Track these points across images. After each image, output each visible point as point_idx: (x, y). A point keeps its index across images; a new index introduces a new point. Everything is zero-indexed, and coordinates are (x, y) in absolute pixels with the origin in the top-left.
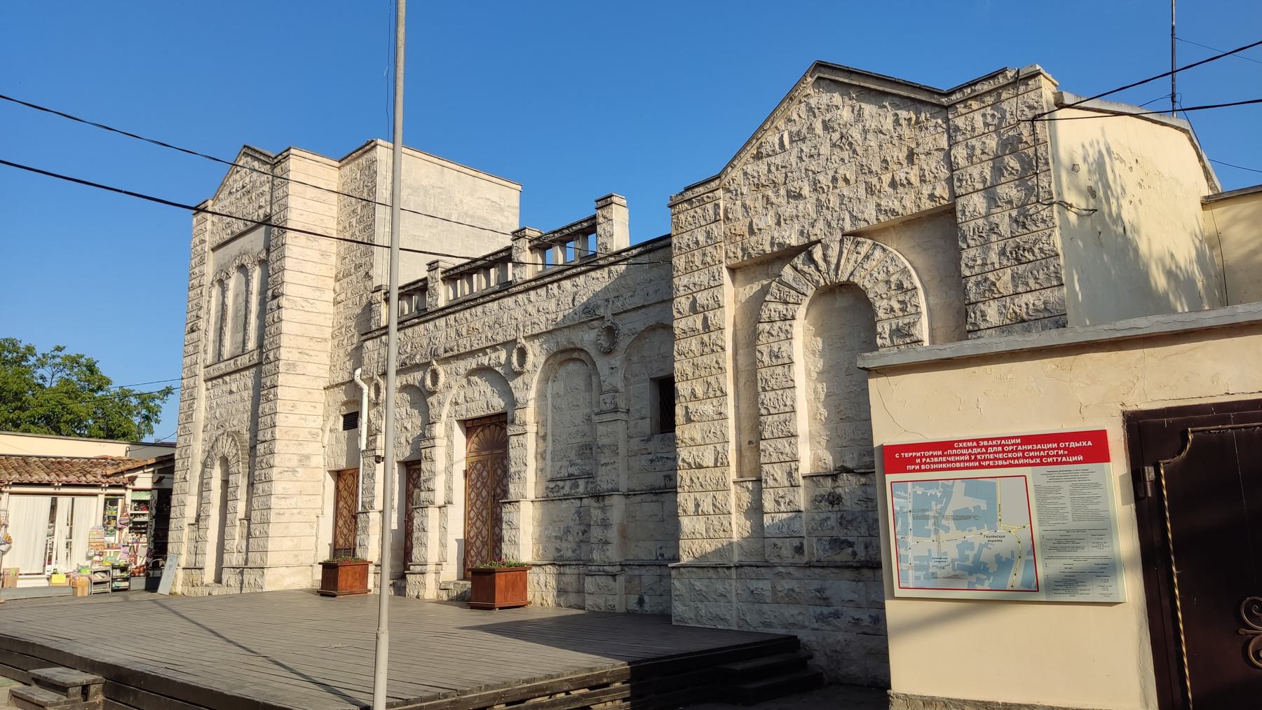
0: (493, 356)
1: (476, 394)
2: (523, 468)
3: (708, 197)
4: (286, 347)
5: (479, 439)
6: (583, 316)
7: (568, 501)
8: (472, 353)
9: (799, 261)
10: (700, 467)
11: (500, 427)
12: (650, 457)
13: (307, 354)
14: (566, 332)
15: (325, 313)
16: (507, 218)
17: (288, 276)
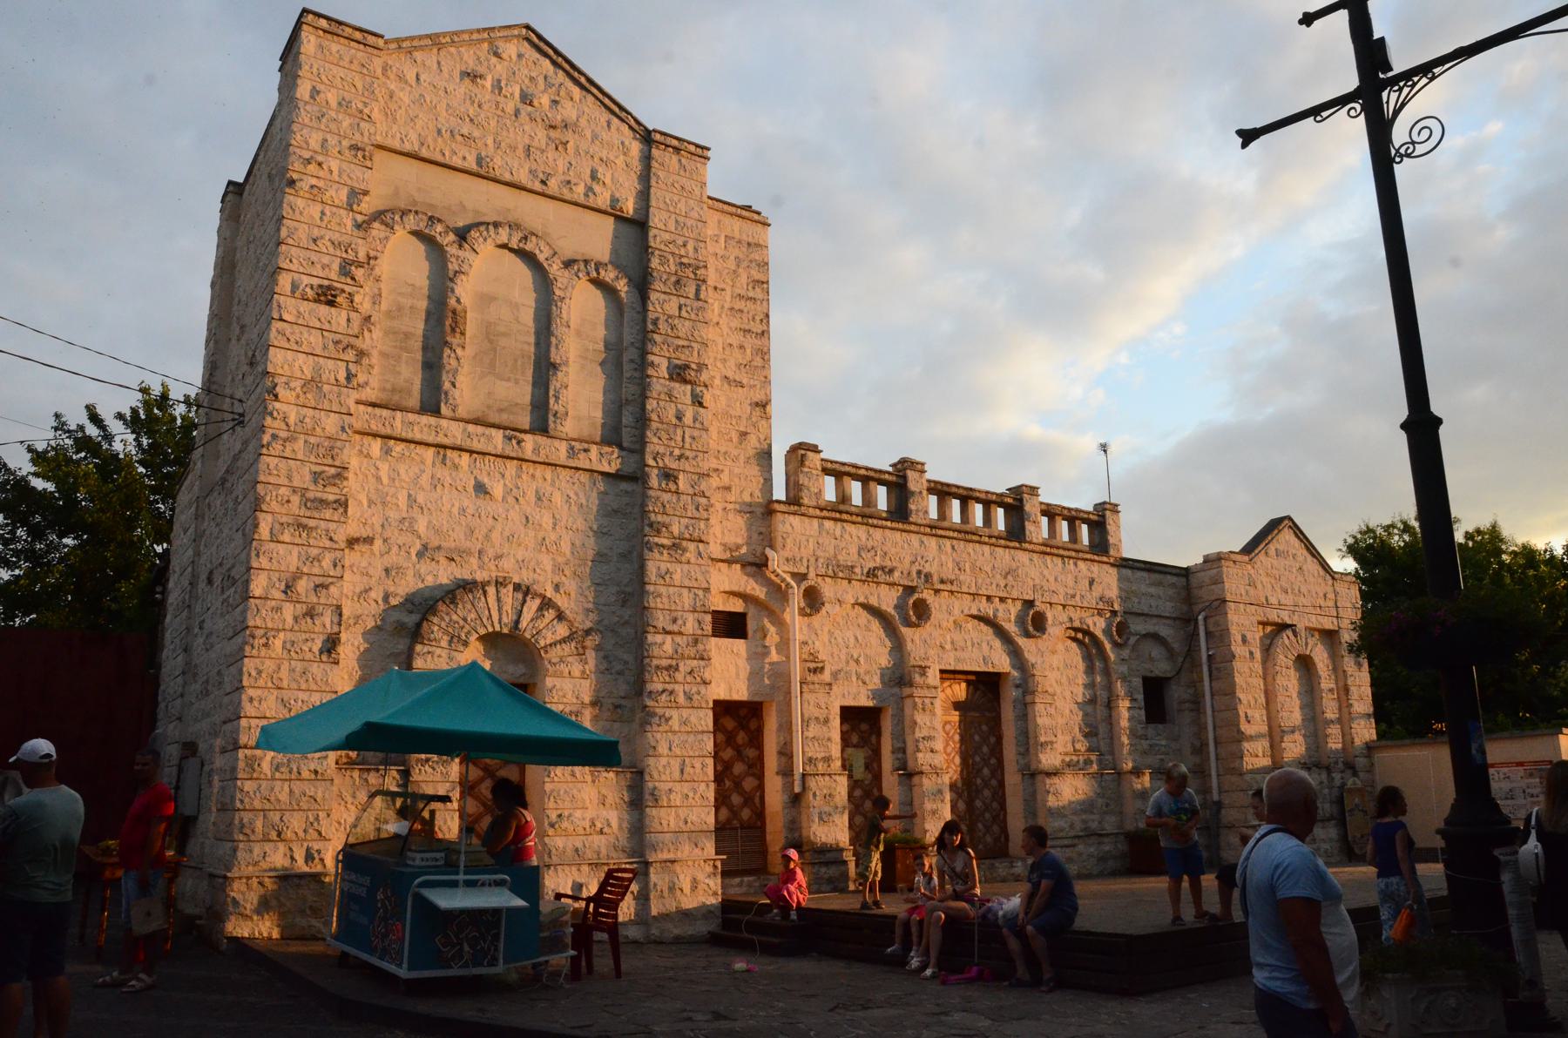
0: (1001, 607)
9: (1289, 632)
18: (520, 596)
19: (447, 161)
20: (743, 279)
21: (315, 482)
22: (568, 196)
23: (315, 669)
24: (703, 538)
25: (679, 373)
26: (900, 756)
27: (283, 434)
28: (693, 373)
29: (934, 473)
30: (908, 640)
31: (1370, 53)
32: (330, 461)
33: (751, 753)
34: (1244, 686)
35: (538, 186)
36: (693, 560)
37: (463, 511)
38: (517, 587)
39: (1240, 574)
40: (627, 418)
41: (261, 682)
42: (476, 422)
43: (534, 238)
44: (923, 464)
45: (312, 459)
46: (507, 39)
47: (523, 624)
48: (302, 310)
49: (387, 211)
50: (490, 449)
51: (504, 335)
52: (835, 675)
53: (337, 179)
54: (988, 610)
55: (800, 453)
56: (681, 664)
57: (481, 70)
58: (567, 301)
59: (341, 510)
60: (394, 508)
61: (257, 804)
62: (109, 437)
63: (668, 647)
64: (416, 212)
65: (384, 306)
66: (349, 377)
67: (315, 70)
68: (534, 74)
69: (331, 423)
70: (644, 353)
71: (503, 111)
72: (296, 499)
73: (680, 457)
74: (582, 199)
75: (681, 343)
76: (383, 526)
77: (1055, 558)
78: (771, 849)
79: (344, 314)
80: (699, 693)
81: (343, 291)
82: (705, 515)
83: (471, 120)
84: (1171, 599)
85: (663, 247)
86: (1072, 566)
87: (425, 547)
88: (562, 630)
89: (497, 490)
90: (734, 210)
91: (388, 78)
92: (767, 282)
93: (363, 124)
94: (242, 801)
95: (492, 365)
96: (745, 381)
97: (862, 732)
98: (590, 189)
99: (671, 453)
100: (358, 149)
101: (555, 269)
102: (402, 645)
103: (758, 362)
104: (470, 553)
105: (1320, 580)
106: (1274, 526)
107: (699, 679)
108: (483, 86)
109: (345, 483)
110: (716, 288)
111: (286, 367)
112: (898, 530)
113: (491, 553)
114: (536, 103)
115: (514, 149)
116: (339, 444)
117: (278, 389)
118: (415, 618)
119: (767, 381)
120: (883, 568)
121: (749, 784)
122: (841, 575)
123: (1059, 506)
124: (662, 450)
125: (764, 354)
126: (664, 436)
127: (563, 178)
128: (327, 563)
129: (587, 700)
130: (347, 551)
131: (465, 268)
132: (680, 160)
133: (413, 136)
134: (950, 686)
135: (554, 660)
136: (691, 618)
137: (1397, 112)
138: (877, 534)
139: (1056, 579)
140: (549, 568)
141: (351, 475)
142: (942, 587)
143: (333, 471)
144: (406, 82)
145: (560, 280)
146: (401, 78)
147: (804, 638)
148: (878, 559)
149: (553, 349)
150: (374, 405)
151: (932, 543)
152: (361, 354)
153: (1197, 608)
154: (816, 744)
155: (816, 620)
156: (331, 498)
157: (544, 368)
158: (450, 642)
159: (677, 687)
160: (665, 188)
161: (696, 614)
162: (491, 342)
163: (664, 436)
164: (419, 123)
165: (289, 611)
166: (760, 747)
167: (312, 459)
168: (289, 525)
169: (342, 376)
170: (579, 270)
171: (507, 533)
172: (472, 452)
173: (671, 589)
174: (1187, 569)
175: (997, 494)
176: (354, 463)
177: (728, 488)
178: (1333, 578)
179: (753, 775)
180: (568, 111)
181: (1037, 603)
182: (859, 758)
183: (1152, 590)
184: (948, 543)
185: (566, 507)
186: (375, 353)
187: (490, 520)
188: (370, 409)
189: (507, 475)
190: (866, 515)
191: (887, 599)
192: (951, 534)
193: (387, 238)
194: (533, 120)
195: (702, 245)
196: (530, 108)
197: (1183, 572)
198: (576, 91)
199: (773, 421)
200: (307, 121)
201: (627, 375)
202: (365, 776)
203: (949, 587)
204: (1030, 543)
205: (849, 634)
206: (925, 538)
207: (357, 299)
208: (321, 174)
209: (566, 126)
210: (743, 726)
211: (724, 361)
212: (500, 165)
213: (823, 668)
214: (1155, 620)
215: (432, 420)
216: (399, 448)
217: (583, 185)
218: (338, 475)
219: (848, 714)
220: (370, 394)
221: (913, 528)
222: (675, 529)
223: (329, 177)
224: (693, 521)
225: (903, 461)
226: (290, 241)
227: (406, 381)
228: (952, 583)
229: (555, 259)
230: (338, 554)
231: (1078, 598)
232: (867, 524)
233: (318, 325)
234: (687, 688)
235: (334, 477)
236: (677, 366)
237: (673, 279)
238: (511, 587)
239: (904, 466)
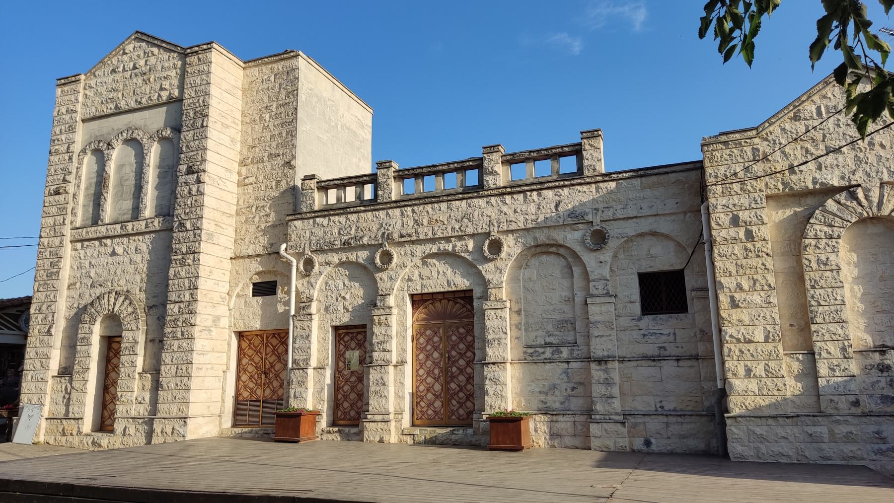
0: (459, 244)
1: (435, 274)
2: (503, 336)
3: (745, 142)
4: (206, 218)
5: (429, 311)
6: (569, 219)
7: (552, 364)
8: (433, 240)
10: (750, 342)
11: (454, 301)
12: (642, 332)
13: (220, 227)
14: (546, 231)
15: (232, 193)
16: (365, 133)
17: (209, 156)
22: (151, 103)
24: (197, 251)
25: (190, 171)
28: (196, 167)
32: (56, 256)
36: (191, 263)
41: (31, 346)
45: (51, 257)
50: (116, 234)
51: (127, 180)
54: (444, 246)
63: (176, 310)
71: (126, 78)
79: (63, 196)
89: (119, 250)
95: (122, 195)
97: (358, 340)
125: (292, 134)
134: (432, 304)
142: (403, 239)
143: (57, 260)
154: (300, 351)
159: (178, 329)
160: (191, 75)
161: (191, 291)
167: (51, 257)
171: (123, 269)
173: (180, 280)
181: (492, 234)
187: (117, 265)
189: (125, 243)
197: (698, 165)
203: (408, 239)
215: (96, 228)
216: (86, 243)
224: (192, 243)
233: (56, 204)
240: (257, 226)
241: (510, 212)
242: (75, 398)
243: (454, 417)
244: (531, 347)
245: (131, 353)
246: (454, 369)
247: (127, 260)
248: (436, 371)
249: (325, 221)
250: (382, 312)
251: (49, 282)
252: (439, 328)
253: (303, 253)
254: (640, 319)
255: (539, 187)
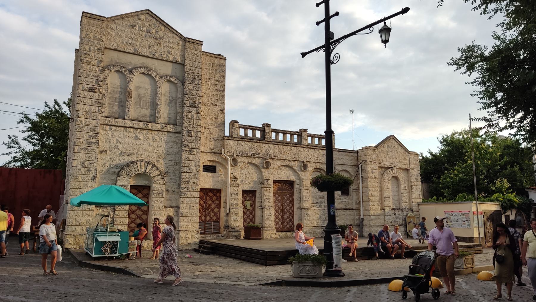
1: (283, 173)
9: (390, 170)
10: (374, 206)
18: (146, 164)
19: (126, 51)
20: (218, 75)
21: (90, 138)
22: (161, 58)
23: (90, 183)
25: (193, 106)
26: (260, 203)
27: (81, 126)
28: (196, 105)
29: (272, 127)
30: (264, 172)
31: (329, 35)
32: (94, 132)
33: (217, 202)
34: (371, 185)
35: (152, 56)
36: (195, 154)
37: (132, 143)
38: (146, 162)
39: (373, 153)
40: (178, 118)
42: (135, 120)
43: (151, 71)
44: (270, 125)
45: (89, 132)
46: (143, 14)
47: (147, 171)
48: (85, 94)
49: (109, 66)
50: (139, 127)
51: (143, 97)
52: (241, 182)
53: (94, 58)
54: (288, 163)
55: (233, 123)
56: (191, 180)
57: (135, 24)
58: (161, 87)
59: (97, 144)
60: (113, 143)
61: (74, 217)
62: (61, 109)
64: (117, 65)
65: (109, 91)
66: (99, 110)
67: (87, 29)
68: (150, 24)
69: (94, 122)
70: (183, 100)
71: (142, 35)
72: (85, 142)
73: (192, 128)
74: (165, 59)
75: (193, 97)
76: (109, 148)
77: (311, 149)
78: (221, 227)
79: (97, 94)
80: (196, 188)
81: (97, 88)
82: (199, 142)
83: (132, 38)
84: (351, 160)
85: (189, 71)
86: (317, 151)
87: (121, 152)
88: (158, 172)
90: (215, 56)
91: (108, 29)
92: (225, 76)
93: (101, 43)
94: (70, 216)
95: (140, 105)
96: (217, 104)
98: (167, 56)
99: (190, 127)
100: (100, 50)
101: (157, 78)
102: (115, 177)
103: (222, 99)
104: (133, 154)
105: (404, 154)
106: (389, 138)
107: (196, 184)
108: (136, 29)
109: (98, 138)
110: (209, 79)
111: (81, 109)
112: (261, 143)
113: (139, 153)
114: (151, 32)
115: (145, 46)
116: (96, 128)
117: (79, 114)
118: (118, 170)
119: (224, 104)
120: (256, 153)
121: (216, 210)
122: (243, 155)
123: (314, 134)
124: (187, 125)
125: (223, 96)
126: (188, 122)
127: (159, 53)
128: (93, 158)
129: (164, 190)
130: (99, 154)
131: (132, 80)
132: (194, 47)
133: (116, 44)
135: (155, 180)
136: (194, 168)
137: (332, 50)
138: (255, 144)
139: (311, 155)
140: (156, 157)
141: (100, 135)
142: (274, 158)
143: (95, 135)
144: (113, 29)
145: (159, 81)
146: (112, 29)
147: (232, 172)
148: (255, 151)
149: (157, 100)
150: (106, 117)
151: (272, 146)
152: (103, 104)
153: (359, 163)
155: (236, 168)
156: (94, 141)
157: (154, 105)
158: (127, 176)
159: (189, 186)
162: (140, 99)
163: (188, 122)
164: (117, 41)
165: (83, 170)
166: (220, 201)
167: (89, 132)
168: (83, 148)
169: (97, 110)
170: (164, 78)
171: (144, 148)
172: (134, 128)
174: (357, 151)
175: (293, 132)
176: (101, 132)
177: (212, 133)
178: (409, 153)
179: (217, 208)
180: (161, 34)
181: (305, 162)
182: (248, 203)
183: (345, 157)
184: (277, 146)
185: (161, 141)
186: (106, 104)
188: (105, 118)
189: (144, 133)
190: (253, 139)
191: (257, 161)
192: (278, 143)
193: (109, 73)
194: (150, 37)
195: (200, 69)
196: (149, 34)
197: (357, 152)
198: (163, 28)
199: (226, 115)
200: (85, 43)
201: (178, 106)
202: (103, 209)
203: (277, 158)
204: (303, 145)
205: (246, 171)
206: (270, 145)
207: (101, 90)
208: (89, 57)
209: (160, 39)
210: (215, 195)
211: (211, 99)
212: (142, 51)
213: (237, 180)
214: (345, 166)
215: (123, 121)
216: (114, 128)
217: (165, 55)
218: (96, 136)
219: (245, 192)
220: (105, 114)
221: (266, 142)
222: (191, 146)
223: (92, 58)
225: (264, 124)
226: (82, 76)
227: (116, 110)
228: (277, 157)
229: (158, 76)
230: (96, 155)
231: (318, 160)
232: (252, 142)
233: (90, 97)
234: (192, 186)
235: (95, 136)
236: (192, 103)
237: (191, 79)
238: (144, 162)
239: (266, 125)
240: (205, 137)
241: (310, 155)
242: (118, 221)
243: (285, 228)
244: (313, 203)
245: (160, 196)
246: (286, 210)
247: (146, 143)
248: (279, 211)
249: (243, 143)
250: (268, 186)
251: (89, 148)
252: (280, 194)
253: (233, 156)
254: (341, 197)
255: (318, 148)
